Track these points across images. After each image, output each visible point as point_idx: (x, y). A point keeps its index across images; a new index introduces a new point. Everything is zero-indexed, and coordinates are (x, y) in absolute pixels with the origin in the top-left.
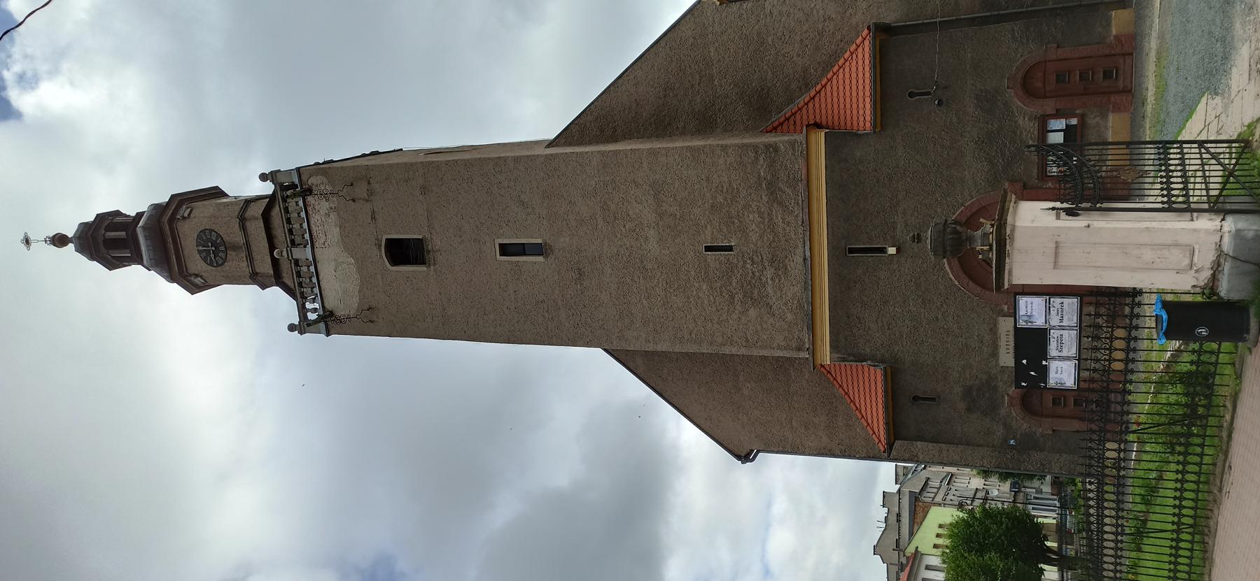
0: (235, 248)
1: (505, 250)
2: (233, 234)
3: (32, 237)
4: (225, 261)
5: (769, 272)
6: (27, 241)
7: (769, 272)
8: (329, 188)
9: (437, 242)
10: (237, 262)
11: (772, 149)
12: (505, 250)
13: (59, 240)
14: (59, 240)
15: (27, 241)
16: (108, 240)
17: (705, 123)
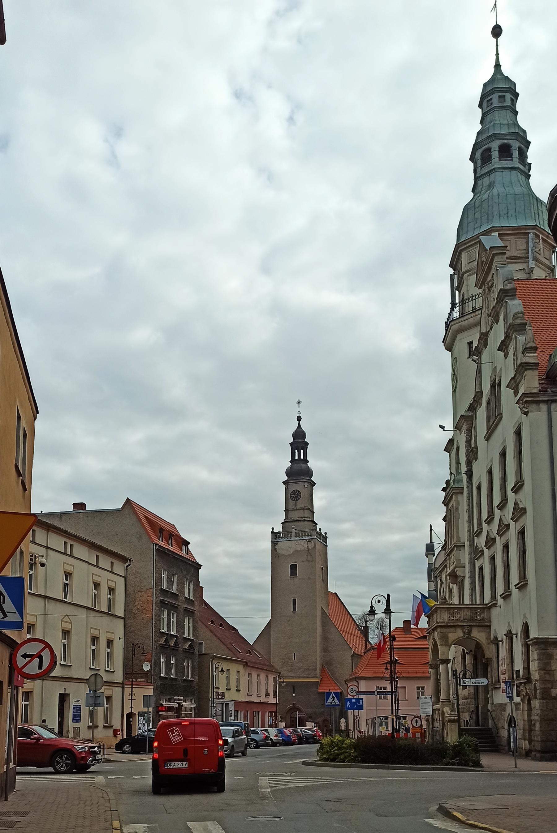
0: (296, 505)
1: (294, 600)
2: (301, 503)
3: (301, 405)
4: (292, 500)
5: (289, 668)
6: (299, 403)
7: (289, 668)
8: (310, 548)
9: (296, 580)
10: (292, 503)
11: (316, 669)
12: (294, 600)
13: (299, 419)
14: (299, 419)
15: (299, 403)
16: (299, 441)
17: (325, 650)
